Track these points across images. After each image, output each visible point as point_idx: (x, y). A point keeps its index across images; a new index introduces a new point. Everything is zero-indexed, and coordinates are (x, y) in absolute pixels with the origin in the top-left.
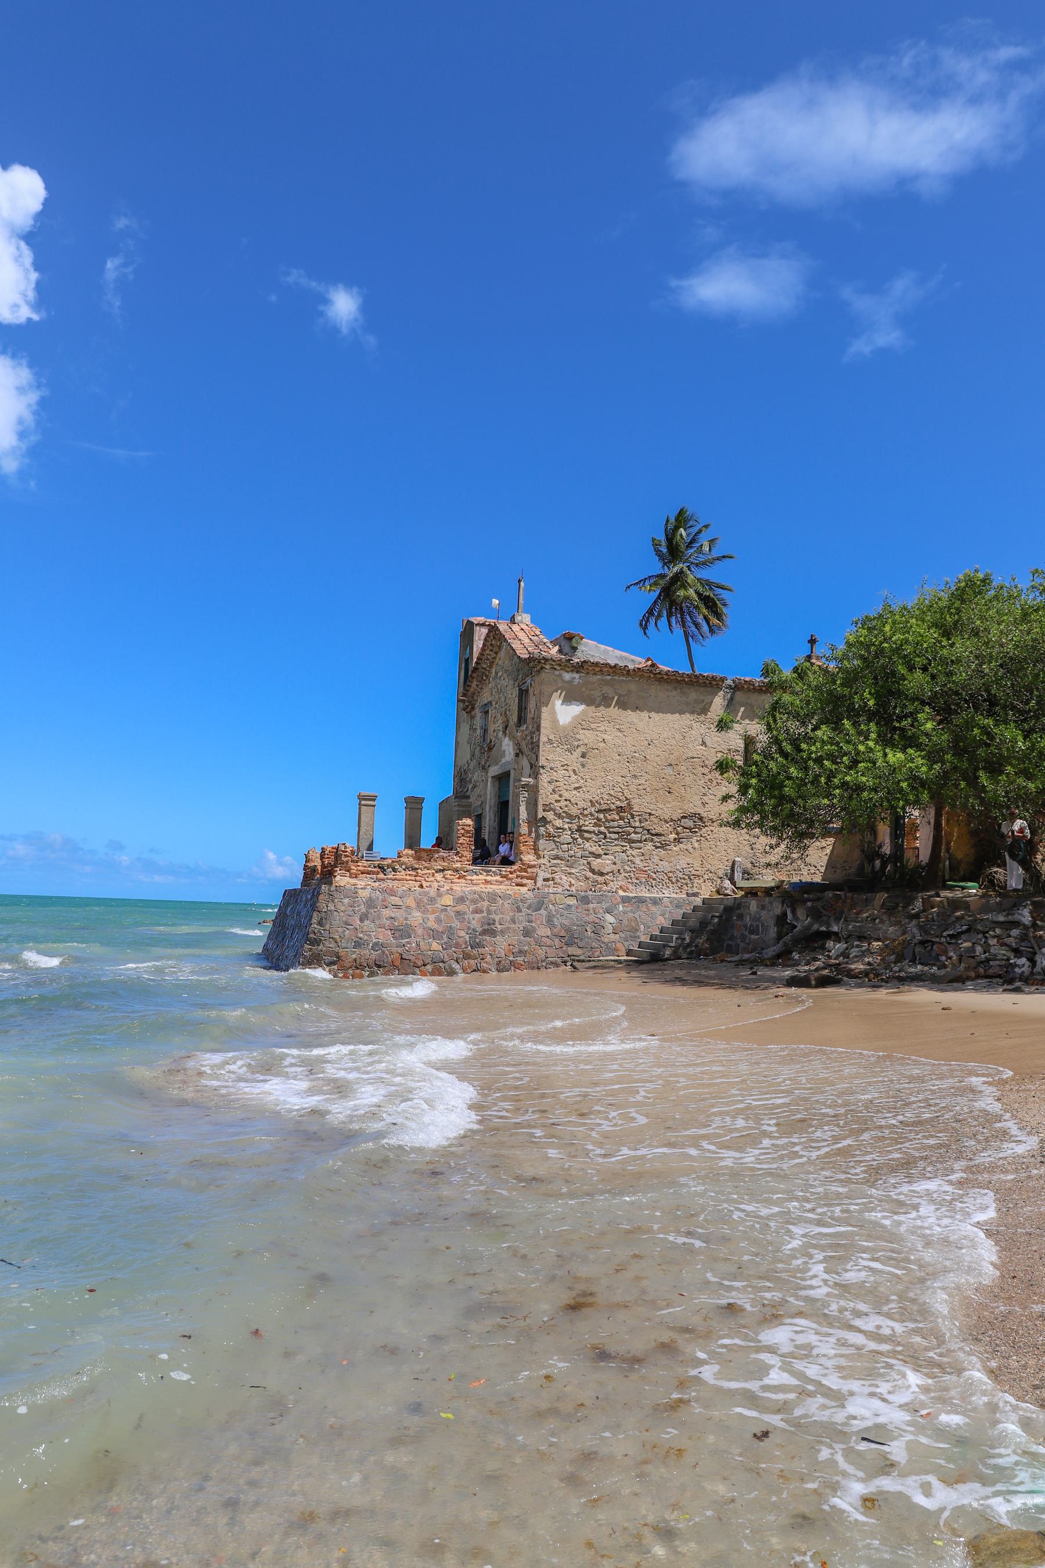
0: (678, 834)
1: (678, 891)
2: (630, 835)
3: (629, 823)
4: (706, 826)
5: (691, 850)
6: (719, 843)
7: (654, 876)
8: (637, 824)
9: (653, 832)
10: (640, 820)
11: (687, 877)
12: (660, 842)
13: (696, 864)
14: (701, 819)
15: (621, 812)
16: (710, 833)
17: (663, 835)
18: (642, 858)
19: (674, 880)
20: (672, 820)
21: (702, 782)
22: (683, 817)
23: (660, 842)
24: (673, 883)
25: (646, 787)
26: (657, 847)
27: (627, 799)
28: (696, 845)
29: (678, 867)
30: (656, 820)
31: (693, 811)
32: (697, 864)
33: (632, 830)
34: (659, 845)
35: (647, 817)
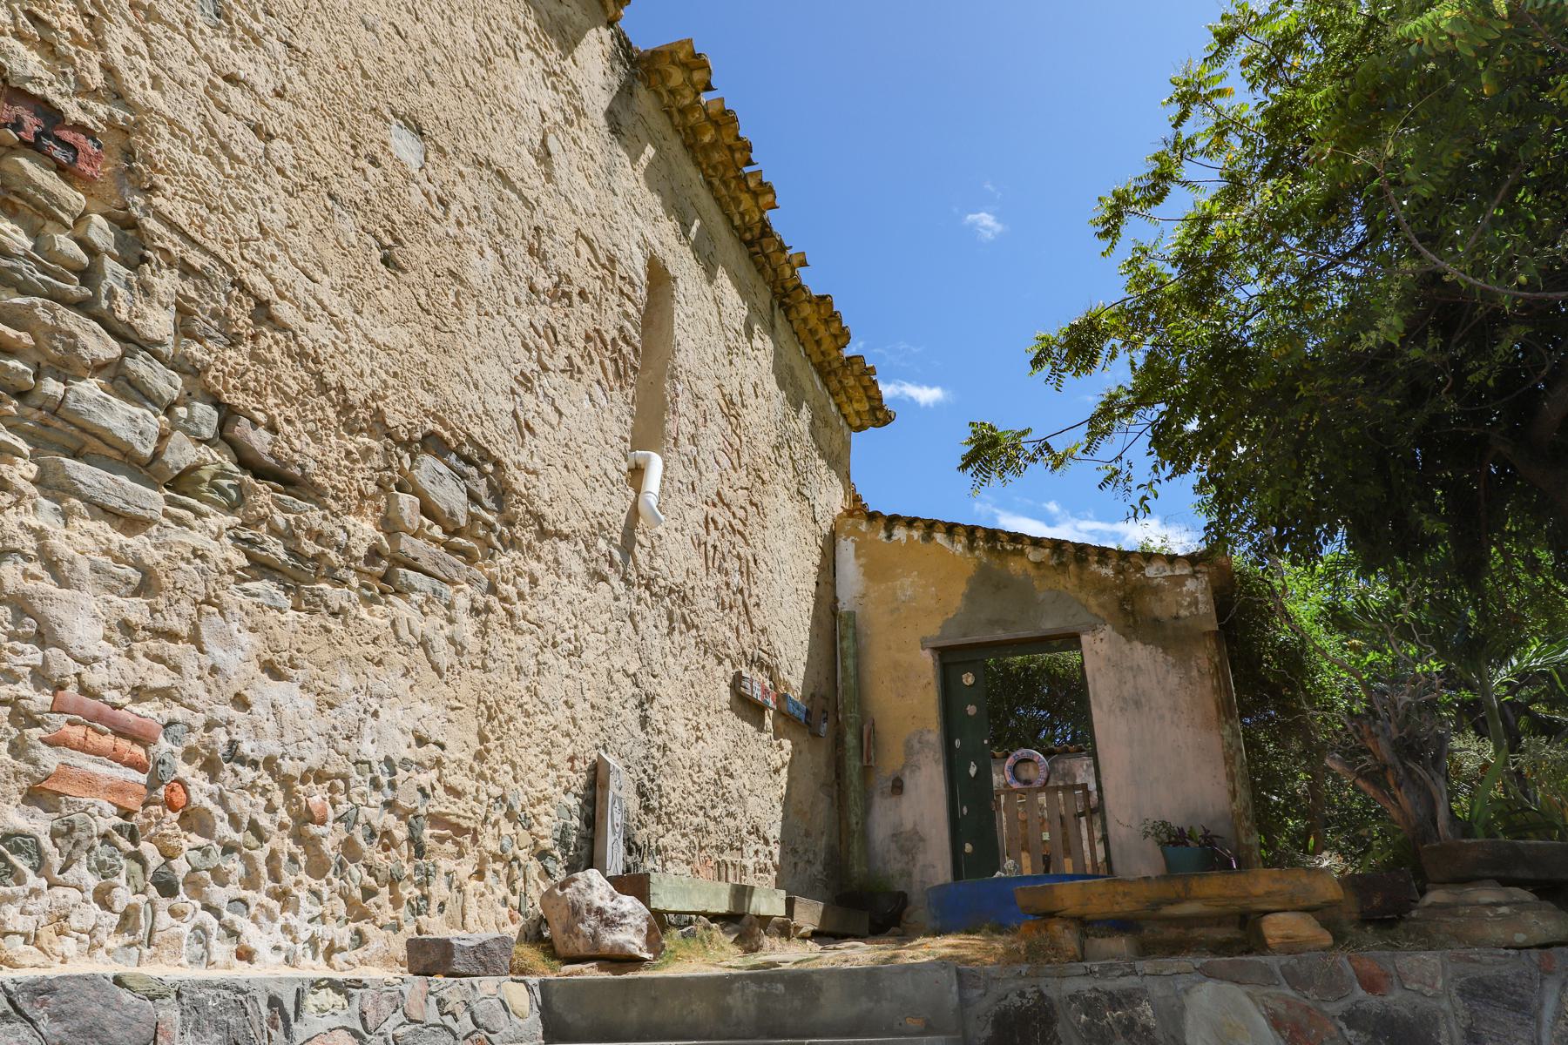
0: (390, 525)
1: (343, 934)
2: (67, 369)
3: (88, 275)
4: (513, 543)
5: (445, 656)
6: (548, 656)
7: (200, 789)
8: (159, 323)
9: (260, 441)
10: (184, 313)
11: (401, 833)
12: (288, 536)
13: (453, 752)
14: (501, 493)
15: (34, 147)
16: (524, 583)
17: (315, 494)
18: (136, 610)
19: (330, 838)
20: (378, 425)
21: (525, 317)
22: (433, 444)
23: (288, 536)
24: (318, 868)
25: (273, 125)
26: (261, 567)
27: (118, 95)
28: (467, 627)
29: (369, 750)
30: (293, 377)
31: (476, 431)
32: (460, 743)
33: (99, 345)
34: (276, 550)
35: (241, 318)
